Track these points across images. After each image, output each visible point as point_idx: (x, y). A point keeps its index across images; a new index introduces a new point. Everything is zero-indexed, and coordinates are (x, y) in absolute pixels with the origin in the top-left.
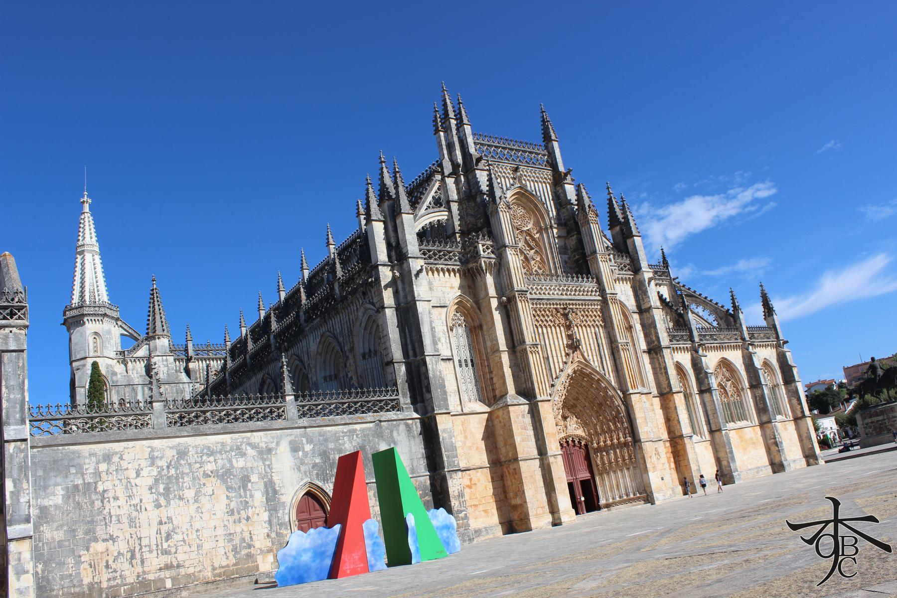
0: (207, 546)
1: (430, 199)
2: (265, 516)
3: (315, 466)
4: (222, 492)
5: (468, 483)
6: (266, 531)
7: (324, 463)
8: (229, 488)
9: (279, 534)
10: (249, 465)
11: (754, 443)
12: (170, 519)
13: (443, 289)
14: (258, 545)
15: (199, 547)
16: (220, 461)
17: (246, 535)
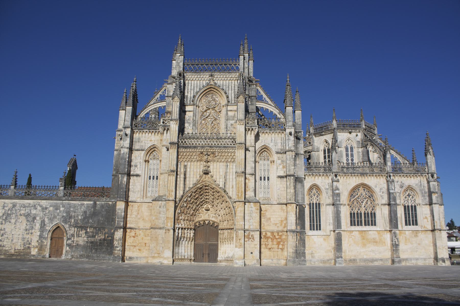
0: (14, 241)
1: (158, 96)
2: (38, 233)
3: (63, 216)
4: (25, 222)
5: (134, 235)
6: (37, 239)
7: (67, 216)
8: (28, 221)
9: (42, 241)
10: (37, 213)
11: (376, 242)
12: (4, 229)
13: (146, 142)
14: (33, 244)
15: (12, 240)
16: (27, 210)
17: (30, 240)
